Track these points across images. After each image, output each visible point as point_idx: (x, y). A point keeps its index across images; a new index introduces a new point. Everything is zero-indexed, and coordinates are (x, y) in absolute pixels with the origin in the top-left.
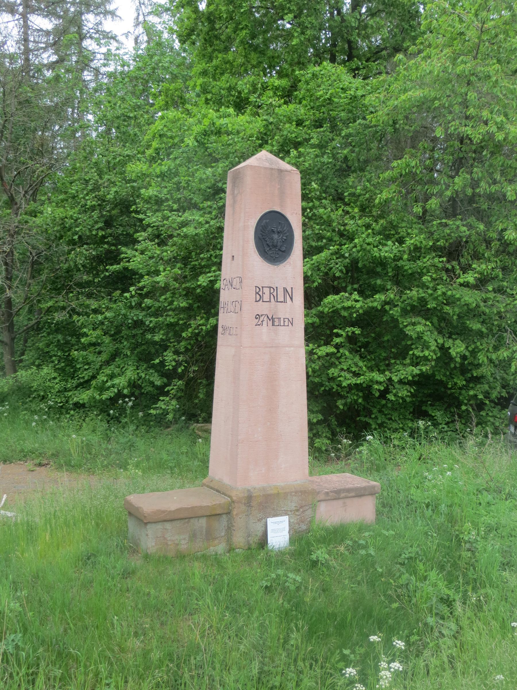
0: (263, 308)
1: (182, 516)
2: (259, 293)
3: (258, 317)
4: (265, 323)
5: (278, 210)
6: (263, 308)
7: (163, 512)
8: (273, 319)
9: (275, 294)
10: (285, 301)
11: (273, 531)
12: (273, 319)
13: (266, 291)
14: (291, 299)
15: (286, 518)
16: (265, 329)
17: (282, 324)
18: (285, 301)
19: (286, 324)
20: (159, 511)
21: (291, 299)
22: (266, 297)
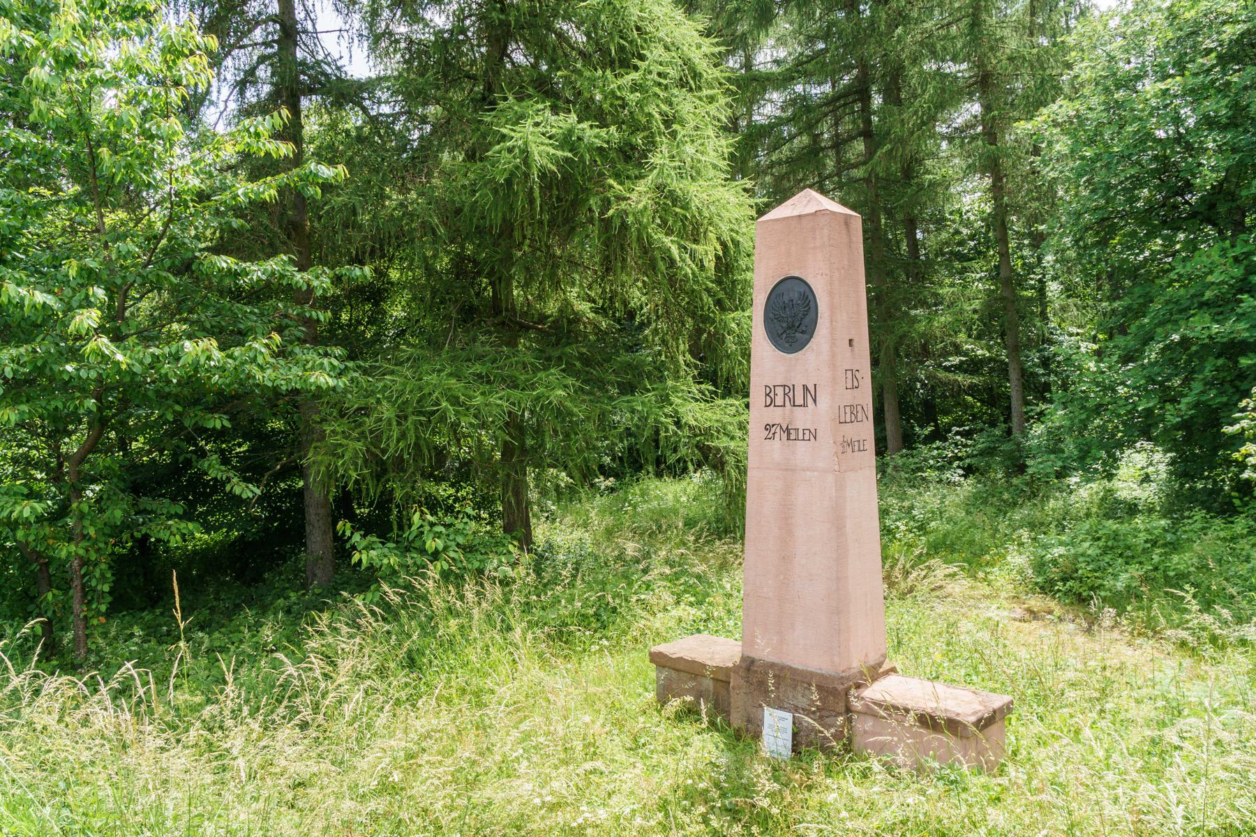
0: (775, 415)
1: (681, 667)
2: (769, 393)
3: (768, 427)
4: (777, 436)
5: (796, 274)
6: (775, 415)
7: (666, 656)
8: (788, 430)
9: (791, 394)
10: (805, 405)
11: (771, 726)
12: (788, 430)
13: (780, 391)
14: (815, 401)
15: (789, 716)
16: (776, 444)
17: (801, 437)
18: (805, 405)
19: (807, 437)
20: (660, 653)
21: (815, 401)
22: (779, 401)
